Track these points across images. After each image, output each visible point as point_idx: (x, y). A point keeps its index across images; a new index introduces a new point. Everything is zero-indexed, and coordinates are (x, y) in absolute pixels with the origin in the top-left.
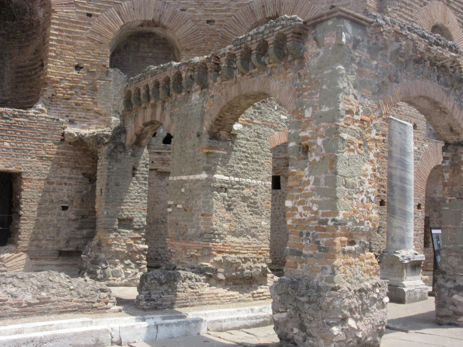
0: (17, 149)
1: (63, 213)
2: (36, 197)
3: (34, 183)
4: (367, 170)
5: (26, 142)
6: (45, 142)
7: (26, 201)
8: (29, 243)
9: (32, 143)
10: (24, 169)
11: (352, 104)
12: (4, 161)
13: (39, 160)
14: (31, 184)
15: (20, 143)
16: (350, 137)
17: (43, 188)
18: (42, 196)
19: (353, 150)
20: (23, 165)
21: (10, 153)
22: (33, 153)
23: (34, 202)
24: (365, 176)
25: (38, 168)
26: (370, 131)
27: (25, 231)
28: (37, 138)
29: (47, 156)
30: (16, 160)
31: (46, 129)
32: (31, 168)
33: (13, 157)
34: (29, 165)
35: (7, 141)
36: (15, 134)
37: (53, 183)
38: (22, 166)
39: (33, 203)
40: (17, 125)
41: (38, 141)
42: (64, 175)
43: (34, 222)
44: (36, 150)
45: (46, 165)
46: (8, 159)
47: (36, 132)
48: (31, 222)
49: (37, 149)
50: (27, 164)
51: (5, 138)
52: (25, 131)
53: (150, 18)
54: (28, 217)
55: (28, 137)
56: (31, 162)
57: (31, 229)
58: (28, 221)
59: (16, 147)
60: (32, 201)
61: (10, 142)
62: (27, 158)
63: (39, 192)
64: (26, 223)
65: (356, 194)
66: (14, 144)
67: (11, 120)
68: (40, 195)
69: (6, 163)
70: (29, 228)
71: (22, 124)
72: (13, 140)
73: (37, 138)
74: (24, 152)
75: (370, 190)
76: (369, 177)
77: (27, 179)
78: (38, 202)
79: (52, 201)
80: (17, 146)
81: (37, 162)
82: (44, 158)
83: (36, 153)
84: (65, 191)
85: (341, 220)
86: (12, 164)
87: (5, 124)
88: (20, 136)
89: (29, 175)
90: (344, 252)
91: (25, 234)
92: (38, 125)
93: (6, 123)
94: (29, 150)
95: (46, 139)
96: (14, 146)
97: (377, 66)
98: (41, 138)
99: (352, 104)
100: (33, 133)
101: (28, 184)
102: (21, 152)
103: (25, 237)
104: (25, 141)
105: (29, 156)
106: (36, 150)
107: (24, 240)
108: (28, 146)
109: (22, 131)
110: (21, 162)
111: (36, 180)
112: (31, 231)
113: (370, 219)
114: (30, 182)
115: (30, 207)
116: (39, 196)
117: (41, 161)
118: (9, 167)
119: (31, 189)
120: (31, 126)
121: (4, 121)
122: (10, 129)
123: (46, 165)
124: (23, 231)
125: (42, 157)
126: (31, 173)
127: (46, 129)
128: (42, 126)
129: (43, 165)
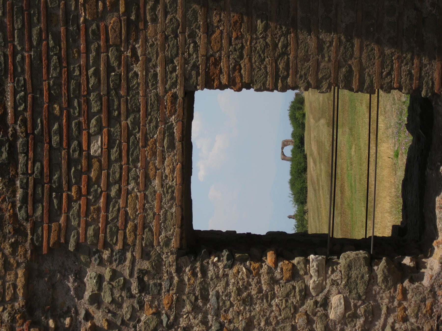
0: (109, 113)
2: (268, 40)
3: (220, 49)
5: (83, 79)
6: (77, 17)
7: (282, 73)
8: (431, 58)
9: (82, 62)
10: (174, 85)
12: (154, 154)
13: (142, 36)
14: (224, 59)
15: (88, 102)
17: (235, 17)
18: (265, 17)
20: (160, 90)
21: (124, 134)
22: (118, 59)
23: (286, 46)
25: (166, 38)
27: (389, 74)
28: (63, 45)
29: (122, 9)
30: (147, 114)
31: (30, 17)
32: (168, 61)
33: (136, 123)
34: (158, 69)
35: (85, 147)
36: (59, 119)
38: (166, 92)
39: (292, 47)
40: (28, 115)
41: (75, 41)
43: (356, 42)
44: (108, 47)
45: (154, 9)
46: (146, 140)
47: (44, 49)
48: (356, 53)
49: (102, 43)
50: (155, 75)
51: (76, 155)
52: (45, 88)
54: (338, 66)
55: (64, 76)
56: (148, 60)
57: (382, 54)
58: (353, 62)
59: (103, 116)
60: (284, 53)
61: (89, 135)
62: (136, 74)
63: (252, 29)
64: (362, 70)
66: (93, 122)
67: (15, 135)
68: (260, 25)
69: (159, 149)
70: (377, 62)
71: (25, 96)
72: (79, 124)
73: (63, 45)
74: (118, 87)
77: (207, 73)
78: (288, 33)
80: (100, 111)
81: (146, 40)
82: (133, 18)
83: (117, 46)
86: (161, 127)
87: (31, 154)
88: (65, 105)
89: (195, 67)
91: (400, 74)
92: (21, 43)
93: (27, 154)
94: (109, 68)
95: (67, 12)
96: (99, 121)
98: (62, 29)
100: (49, 59)
101: (225, 70)
102: (119, 97)
103: (410, 73)
104: (79, 85)
105: (128, 69)
106: (108, 47)
107: (420, 78)
108: (97, 73)
109: (45, 98)
110: (152, 95)
111: (209, 42)
112: (387, 51)
114: (217, 63)
115: (306, 59)
116: (266, 28)
117: (141, 26)
118: (172, 135)
119: (241, 57)
120: (26, 67)
121: (21, 159)
122: (46, 136)
123: (154, 9)
124: (388, 80)
125: (129, 22)
126: (186, 62)
127: (30, 17)
128: (21, 30)
129: (154, 20)
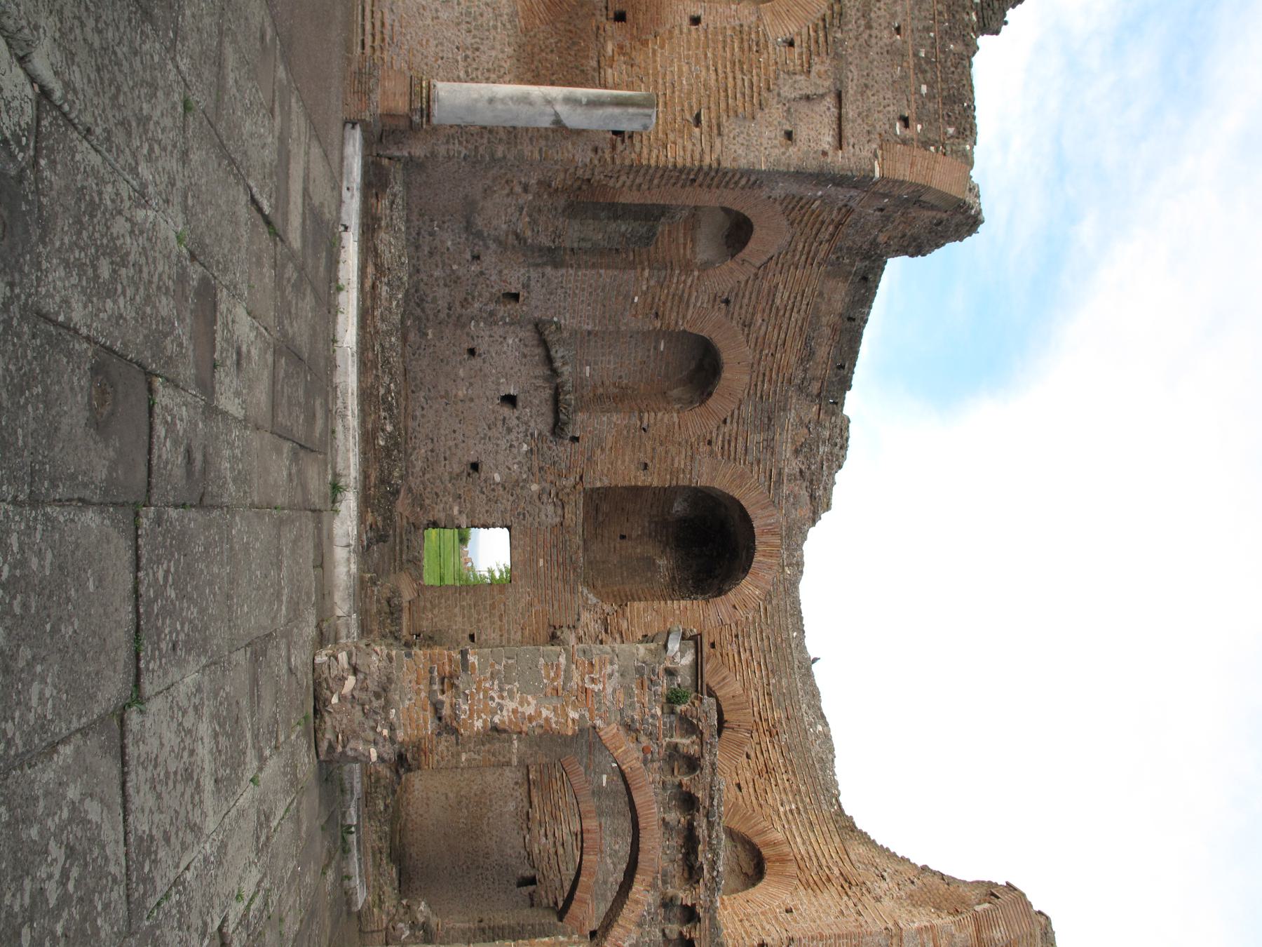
1: (466, 636)
4: (529, 704)
11: (601, 669)
16: (563, 667)
19: (548, 677)
24: (521, 704)
26: (575, 708)
37: (501, 621)
42: (512, 632)
53: (726, 717)
65: (500, 687)
75: (505, 713)
76: (520, 709)
79: (479, 621)
84: (493, 635)
85: (468, 661)
90: (431, 671)
97: (653, 716)
99: (601, 669)
113: (471, 717)
